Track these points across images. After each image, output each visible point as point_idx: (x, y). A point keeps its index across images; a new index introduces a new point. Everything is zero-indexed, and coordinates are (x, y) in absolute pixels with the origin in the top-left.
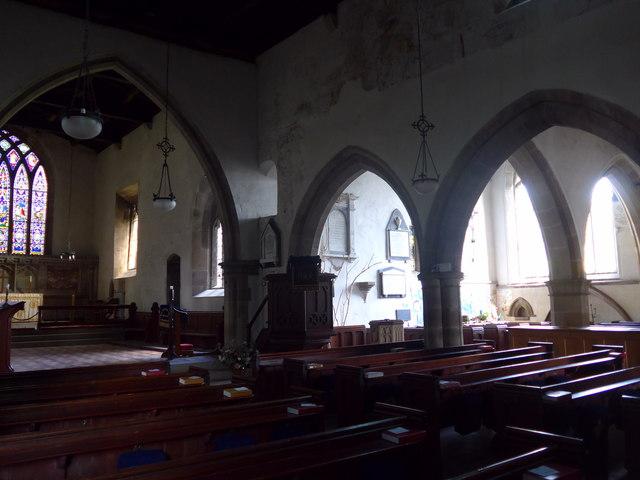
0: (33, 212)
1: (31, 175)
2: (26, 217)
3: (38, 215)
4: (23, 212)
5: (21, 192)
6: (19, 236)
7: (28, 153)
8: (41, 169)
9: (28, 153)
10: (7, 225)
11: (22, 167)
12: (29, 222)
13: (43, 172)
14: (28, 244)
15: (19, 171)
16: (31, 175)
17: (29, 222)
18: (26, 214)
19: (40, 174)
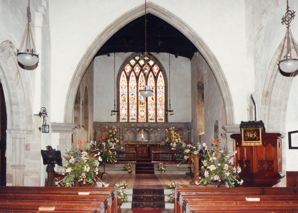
0: (158, 98)
1: (156, 78)
2: (154, 102)
3: (160, 100)
4: (153, 99)
6: (152, 112)
7: (153, 66)
8: (161, 74)
9: (153, 66)
10: (145, 106)
11: (151, 74)
12: (156, 104)
13: (162, 75)
14: (156, 116)
15: (150, 76)
16: (156, 78)
17: (156, 104)
18: (154, 99)
19: (161, 76)
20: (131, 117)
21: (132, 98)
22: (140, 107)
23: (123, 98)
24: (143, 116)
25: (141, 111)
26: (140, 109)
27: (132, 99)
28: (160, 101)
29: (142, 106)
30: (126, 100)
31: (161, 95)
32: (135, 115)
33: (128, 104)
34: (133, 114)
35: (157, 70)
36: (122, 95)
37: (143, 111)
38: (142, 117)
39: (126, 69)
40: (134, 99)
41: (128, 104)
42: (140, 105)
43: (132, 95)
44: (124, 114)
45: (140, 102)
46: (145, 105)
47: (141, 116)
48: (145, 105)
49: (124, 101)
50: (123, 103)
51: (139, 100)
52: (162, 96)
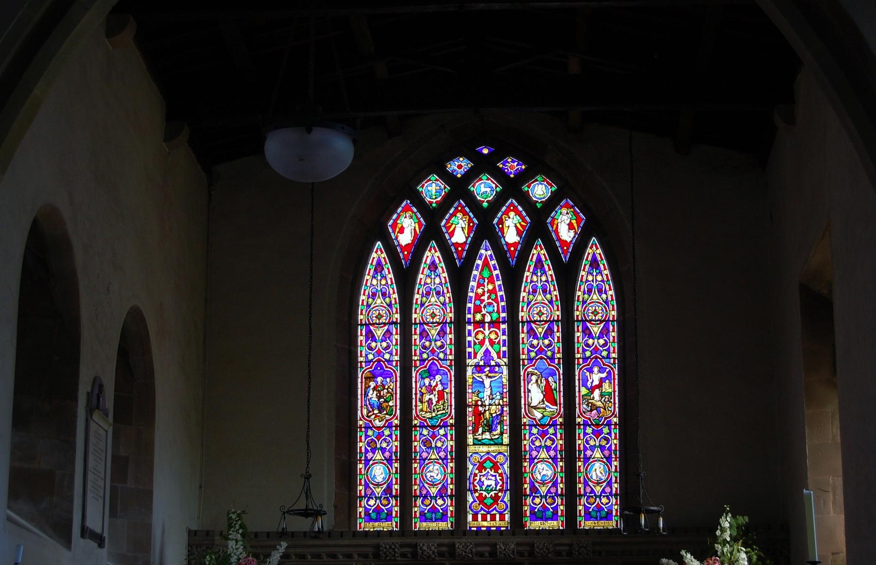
4: (548, 395)
5: (540, 330)
7: (551, 204)
10: (506, 439)
12: (570, 426)
18: (560, 397)
20: (419, 502)
21: (431, 390)
22: (478, 443)
23: (373, 395)
24: (496, 499)
25: (481, 467)
26: (475, 451)
27: (427, 397)
28: (593, 407)
29: (487, 436)
30: (395, 403)
31: (596, 369)
32: (441, 494)
33: (406, 428)
34: (433, 485)
35: (571, 226)
36: (373, 376)
37: (495, 467)
38: (489, 501)
39: (395, 224)
40: (441, 395)
41: (406, 428)
42: (475, 431)
43: (431, 374)
44: (378, 485)
45: (478, 415)
46: (502, 434)
47: (481, 499)
48: (502, 434)
49: (381, 409)
50: (377, 423)
51: (471, 399)
52: (604, 375)
